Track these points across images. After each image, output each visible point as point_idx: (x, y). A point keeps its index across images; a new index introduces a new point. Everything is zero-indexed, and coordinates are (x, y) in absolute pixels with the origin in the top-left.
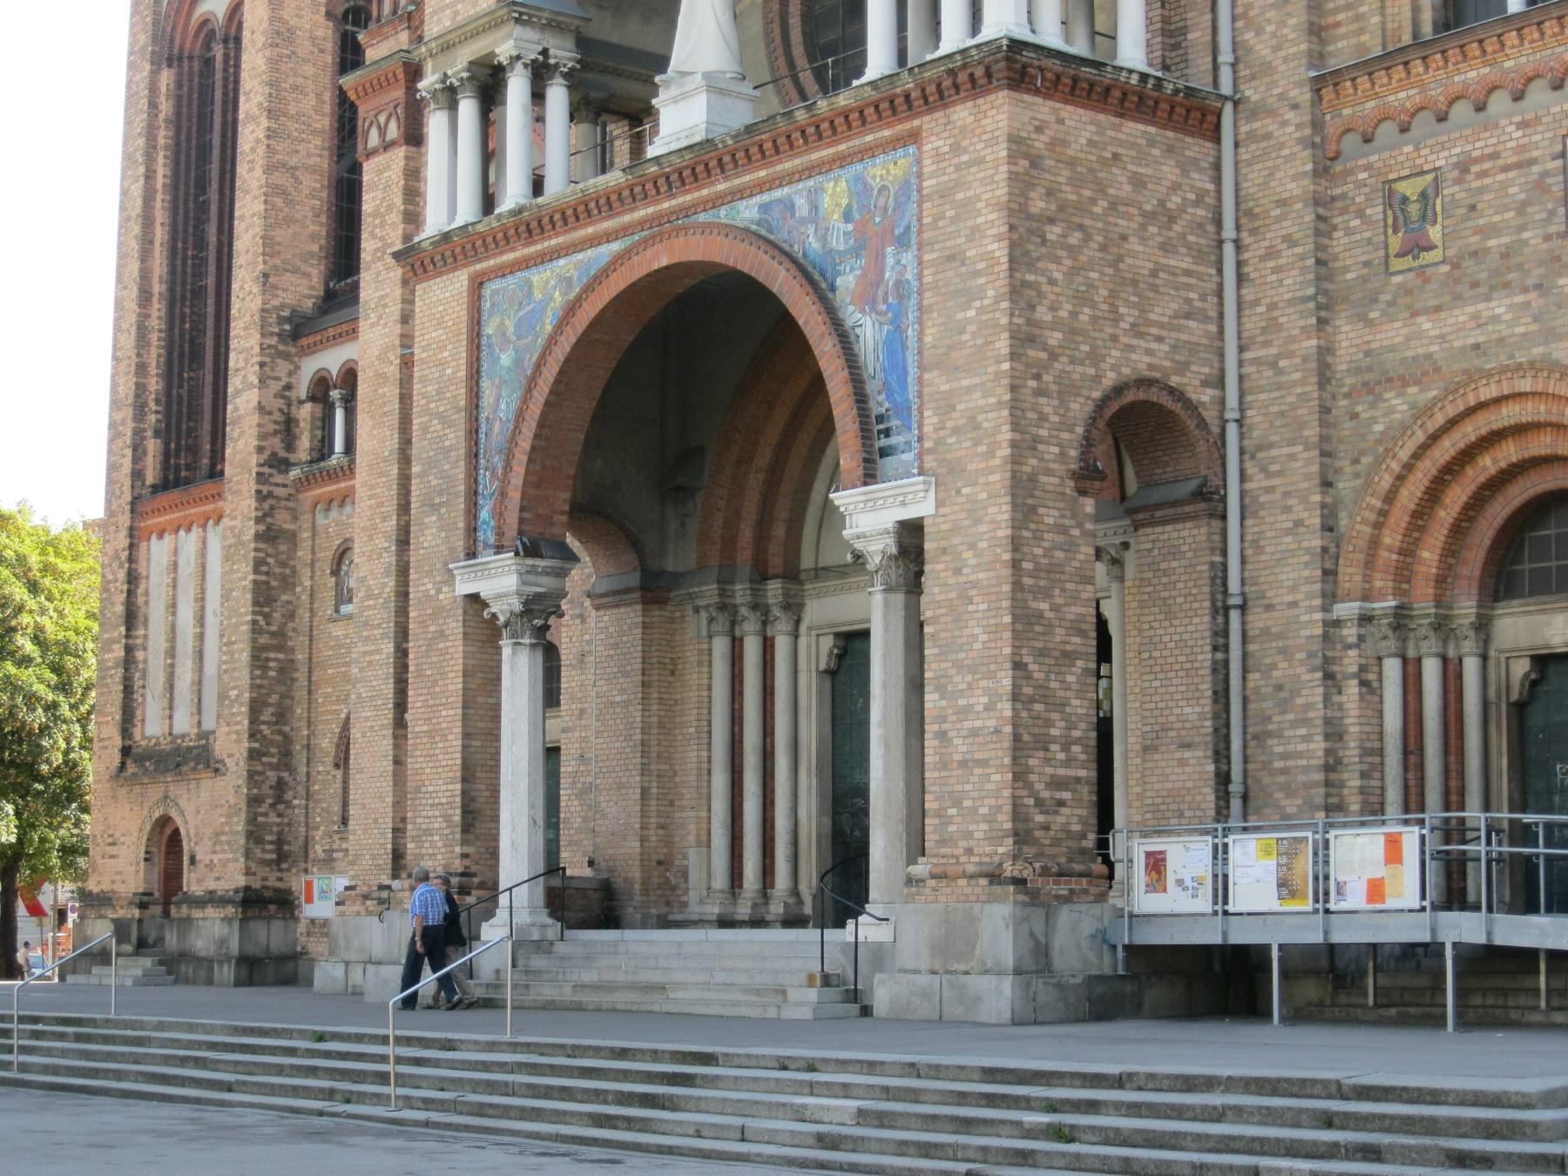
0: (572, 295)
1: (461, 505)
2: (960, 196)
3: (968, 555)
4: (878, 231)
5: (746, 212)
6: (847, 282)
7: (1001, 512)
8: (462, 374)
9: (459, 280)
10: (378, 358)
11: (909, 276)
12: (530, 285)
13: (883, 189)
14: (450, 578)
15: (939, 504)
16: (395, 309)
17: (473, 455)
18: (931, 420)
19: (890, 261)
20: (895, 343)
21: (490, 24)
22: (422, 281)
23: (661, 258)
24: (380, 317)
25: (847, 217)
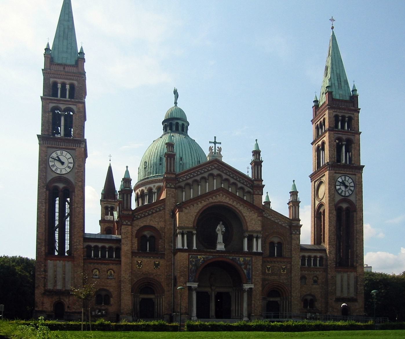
0: (205, 259)
1: (188, 277)
2: (257, 263)
3: (257, 291)
4: (246, 263)
5: (231, 258)
6: (243, 267)
7: (261, 288)
8: (187, 263)
9: (187, 254)
10: (127, 250)
11: (250, 268)
12: (198, 257)
13: (247, 260)
14: (186, 284)
15: (254, 287)
16: (129, 245)
17: (189, 272)
18: (253, 280)
19: (248, 266)
20: (249, 273)
21: (191, 228)
22: (179, 252)
23: (220, 259)
24: (127, 246)
25: (243, 261)
